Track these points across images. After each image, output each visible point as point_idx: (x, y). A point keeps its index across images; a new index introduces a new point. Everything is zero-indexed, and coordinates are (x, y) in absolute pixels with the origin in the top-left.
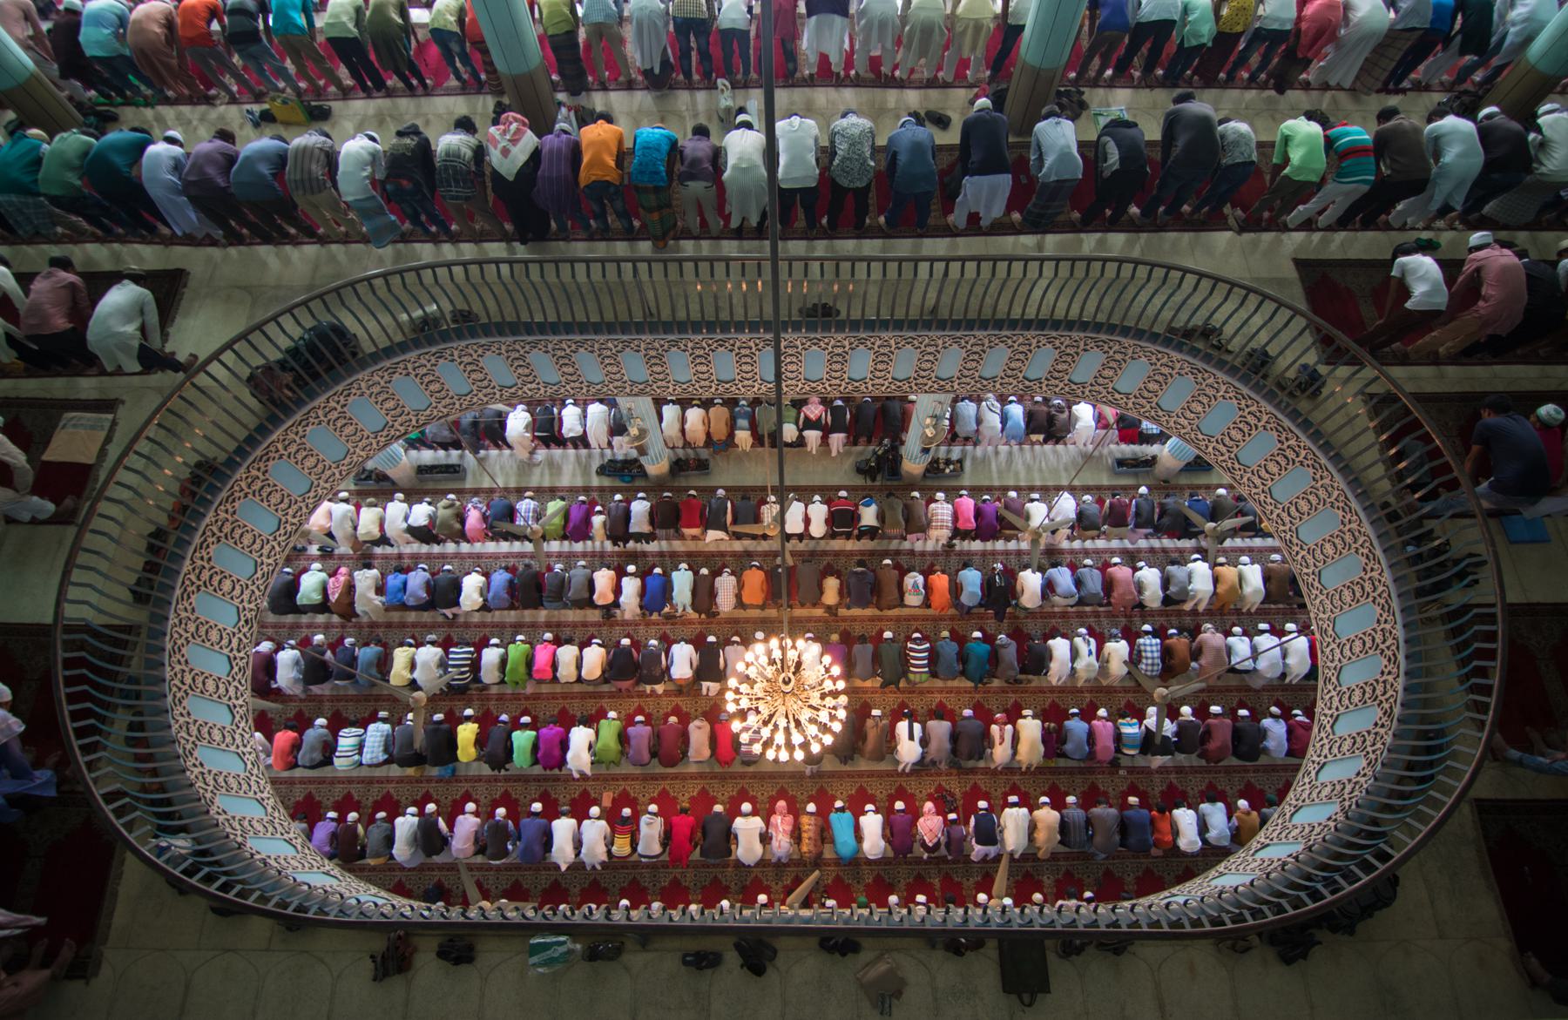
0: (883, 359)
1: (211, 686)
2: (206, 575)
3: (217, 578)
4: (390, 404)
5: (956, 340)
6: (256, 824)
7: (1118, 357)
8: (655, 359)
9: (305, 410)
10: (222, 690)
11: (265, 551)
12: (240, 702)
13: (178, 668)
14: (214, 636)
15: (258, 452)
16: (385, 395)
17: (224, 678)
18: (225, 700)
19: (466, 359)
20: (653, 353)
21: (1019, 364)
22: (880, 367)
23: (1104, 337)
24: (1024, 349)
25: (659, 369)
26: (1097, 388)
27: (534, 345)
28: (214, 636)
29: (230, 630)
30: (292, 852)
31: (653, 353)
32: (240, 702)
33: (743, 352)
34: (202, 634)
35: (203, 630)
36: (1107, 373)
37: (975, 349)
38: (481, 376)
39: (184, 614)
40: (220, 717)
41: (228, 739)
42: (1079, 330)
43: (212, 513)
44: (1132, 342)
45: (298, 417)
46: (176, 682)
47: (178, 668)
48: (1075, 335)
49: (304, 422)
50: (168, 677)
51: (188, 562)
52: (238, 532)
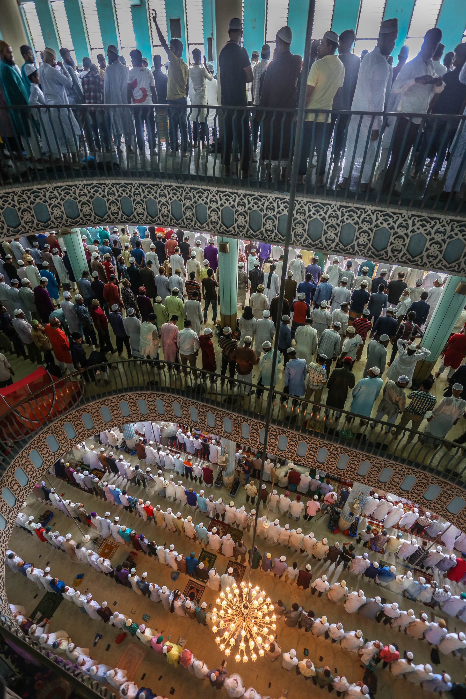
0: (333, 455)
2: (41, 443)
4: (134, 408)
5: (369, 458)
7: (449, 492)
8: (237, 425)
10: (18, 491)
12: (21, 500)
13: (10, 474)
15: (82, 407)
16: (133, 404)
19: (167, 401)
20: (236, 422)
21: (398, 480)
22: (331, 459)
23: (442, 479)
24: (402, 473)
25: (237, 429)
26: (437, 505)
27: (193, 403)
28: (29, 469)
29: (35, 469)
31: (236, 422)
32: (21, 500)
33: (273, 433)
35: (27, 464)
36: (442, 498)
37: (377, 465)
38: (169, 409)
39: (24, 454)
41: (7, 513)
42: (428, 471)
43: (55, 422)
44: (457, 486)
45: (101, 400)
46: (5, 479)
47: (10, 474)
48: (427, 473)
49: (102, 403)
51: (38, 436)
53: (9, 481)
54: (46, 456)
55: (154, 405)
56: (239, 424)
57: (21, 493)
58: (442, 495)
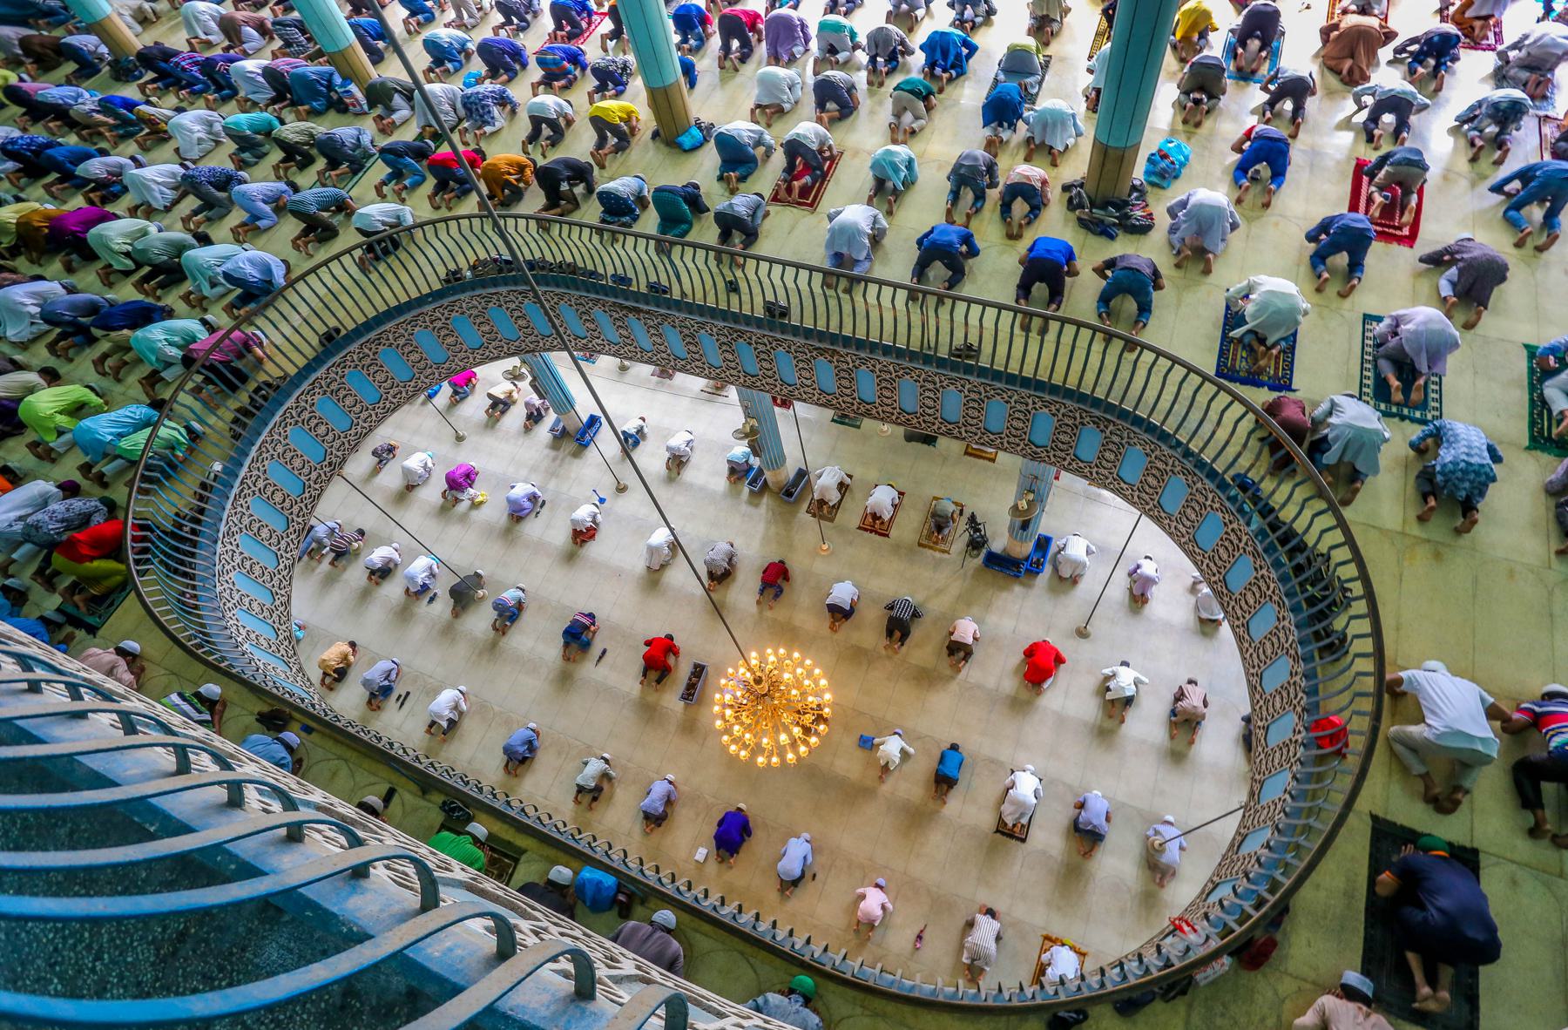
1: (278, 497)
2: (306, 415)
3: (313, 422)
4: (486, 328)
6: (255, 605)
9: (415, 312)
10: (287, 504)
11: (364, 415)
13: (255, 473)
14: (297, 463)
16: (481, 319)
17: (293, 497)
18: (286, 513)
28: (297, 463)
30: (272, 636)
31: (686, 331)
33: (761, 348)
34: (287, 458)
35: (289, 455)
36: (1107, 454)
40: (278, 524)
47: (255, 473)
50: (242, 474)
52: (342, 393)
53: (261, 484)
54: (330, 437)
55: (523, 317)
56: (693, 336)
57: (296, 509)
58: (1105, 447)
